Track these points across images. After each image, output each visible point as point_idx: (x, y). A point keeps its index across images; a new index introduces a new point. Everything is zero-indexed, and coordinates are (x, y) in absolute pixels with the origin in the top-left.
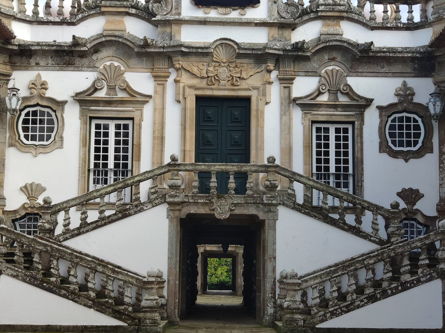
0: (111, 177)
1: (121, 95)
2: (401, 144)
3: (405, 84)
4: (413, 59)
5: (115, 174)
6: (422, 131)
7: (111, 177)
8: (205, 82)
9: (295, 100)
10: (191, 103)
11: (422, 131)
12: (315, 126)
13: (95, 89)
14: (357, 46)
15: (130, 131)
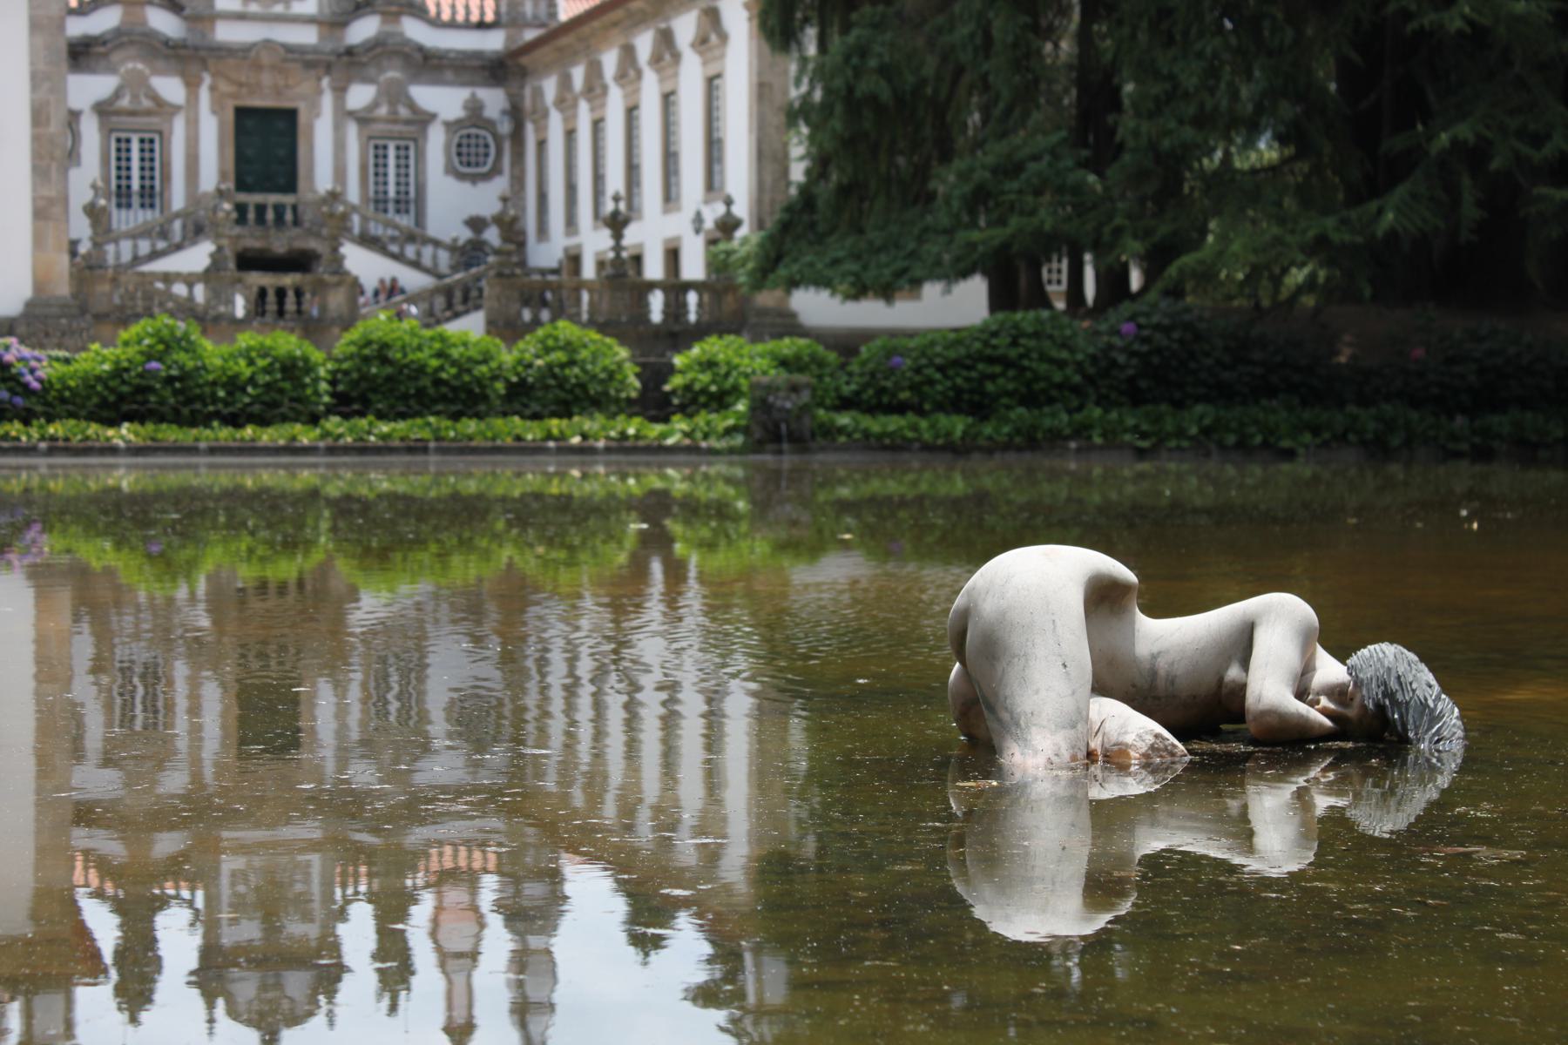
0: (136, 200)
1: (146, 103)
2: (469, 164)
3: (473, 95)
4: (483, 68)
5: (142, 196)
6: (492, 150)
7: (136, 200)
8: (244, 90)
9: (351, 114)
10: (230, 116)
11: (492, 150)
12: (372, 143)
13: (117, 94)
14: (420, 49)
15: (157, 146)
